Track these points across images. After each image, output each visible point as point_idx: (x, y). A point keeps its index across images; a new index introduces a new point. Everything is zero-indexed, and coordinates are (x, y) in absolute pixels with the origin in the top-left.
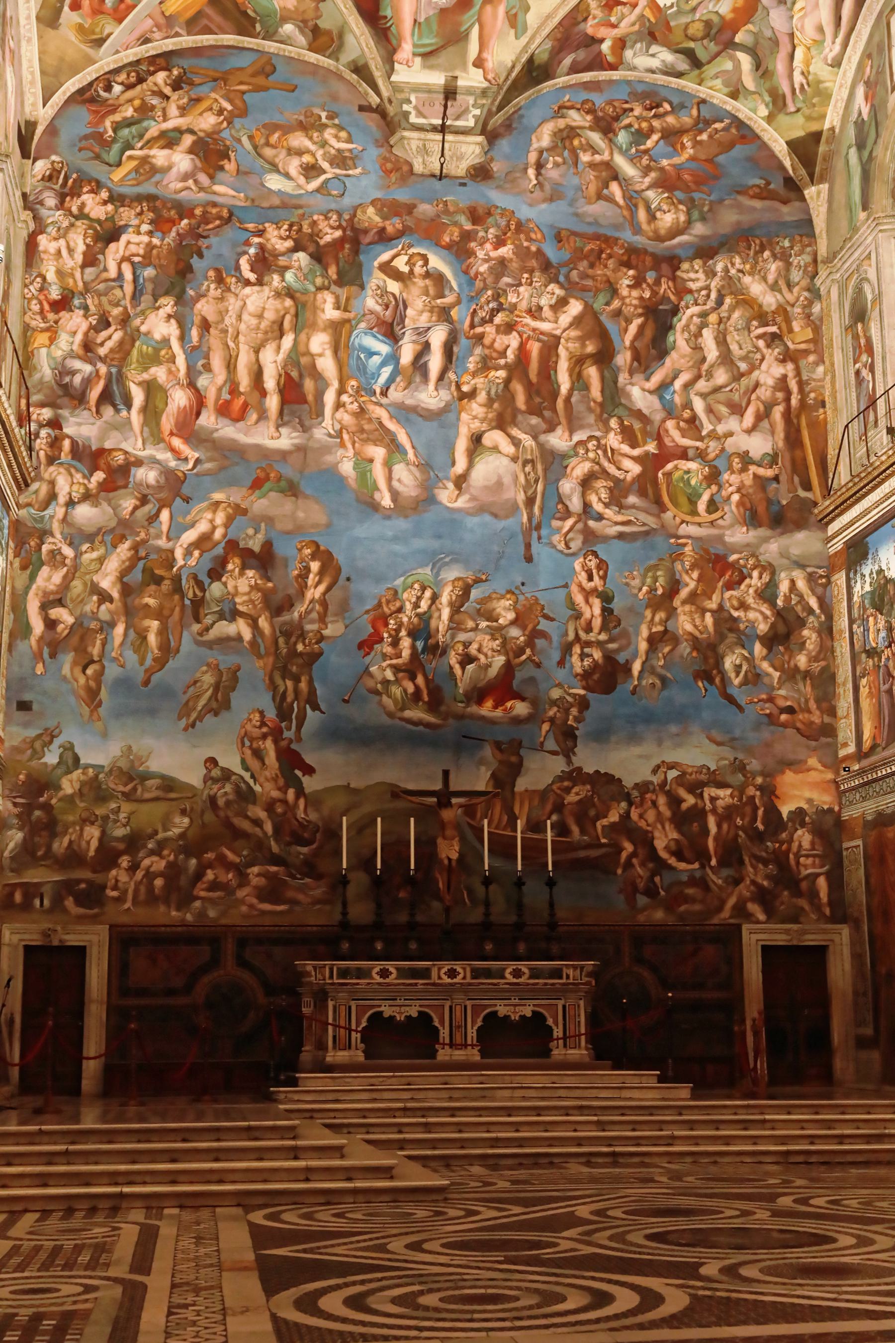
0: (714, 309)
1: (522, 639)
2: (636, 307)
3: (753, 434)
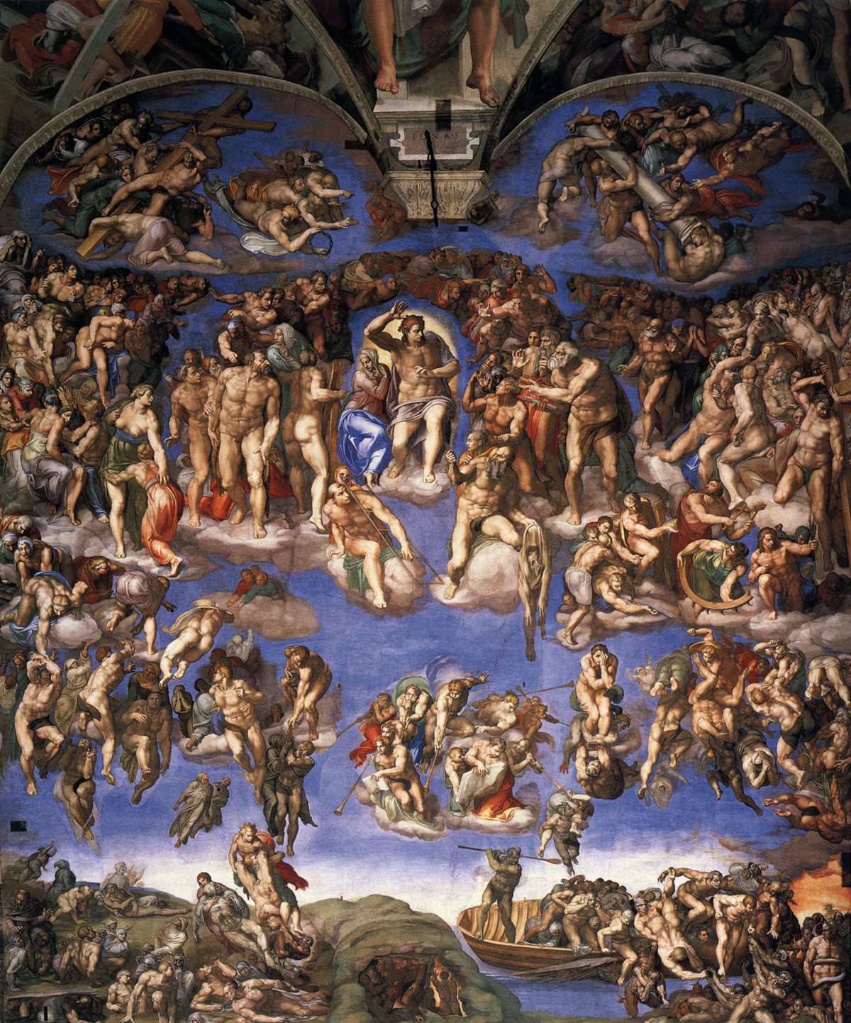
0: (750, 361)
1: (523, 743)
2: (658, 363)
3: (788, 505)
